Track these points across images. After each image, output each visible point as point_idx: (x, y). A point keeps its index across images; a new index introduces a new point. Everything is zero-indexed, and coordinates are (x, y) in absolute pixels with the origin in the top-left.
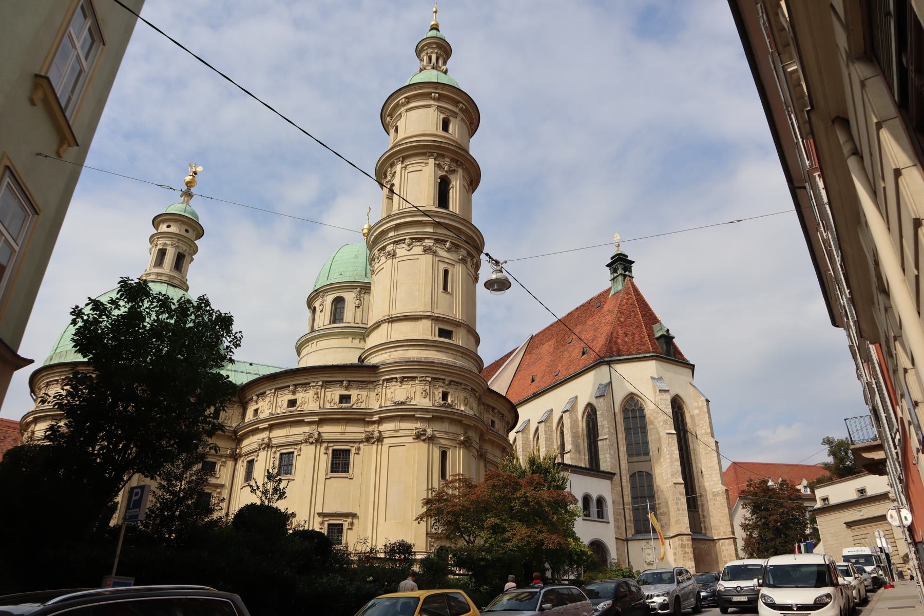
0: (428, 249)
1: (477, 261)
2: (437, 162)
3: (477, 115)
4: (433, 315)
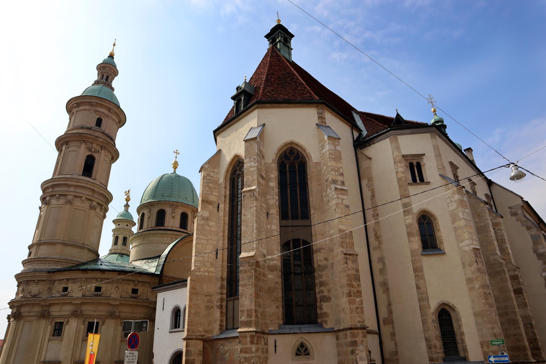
0: (68, 202)
1: (105, 207)
2: (87, 146)
3: (123, 114)
4: (64, 242)
